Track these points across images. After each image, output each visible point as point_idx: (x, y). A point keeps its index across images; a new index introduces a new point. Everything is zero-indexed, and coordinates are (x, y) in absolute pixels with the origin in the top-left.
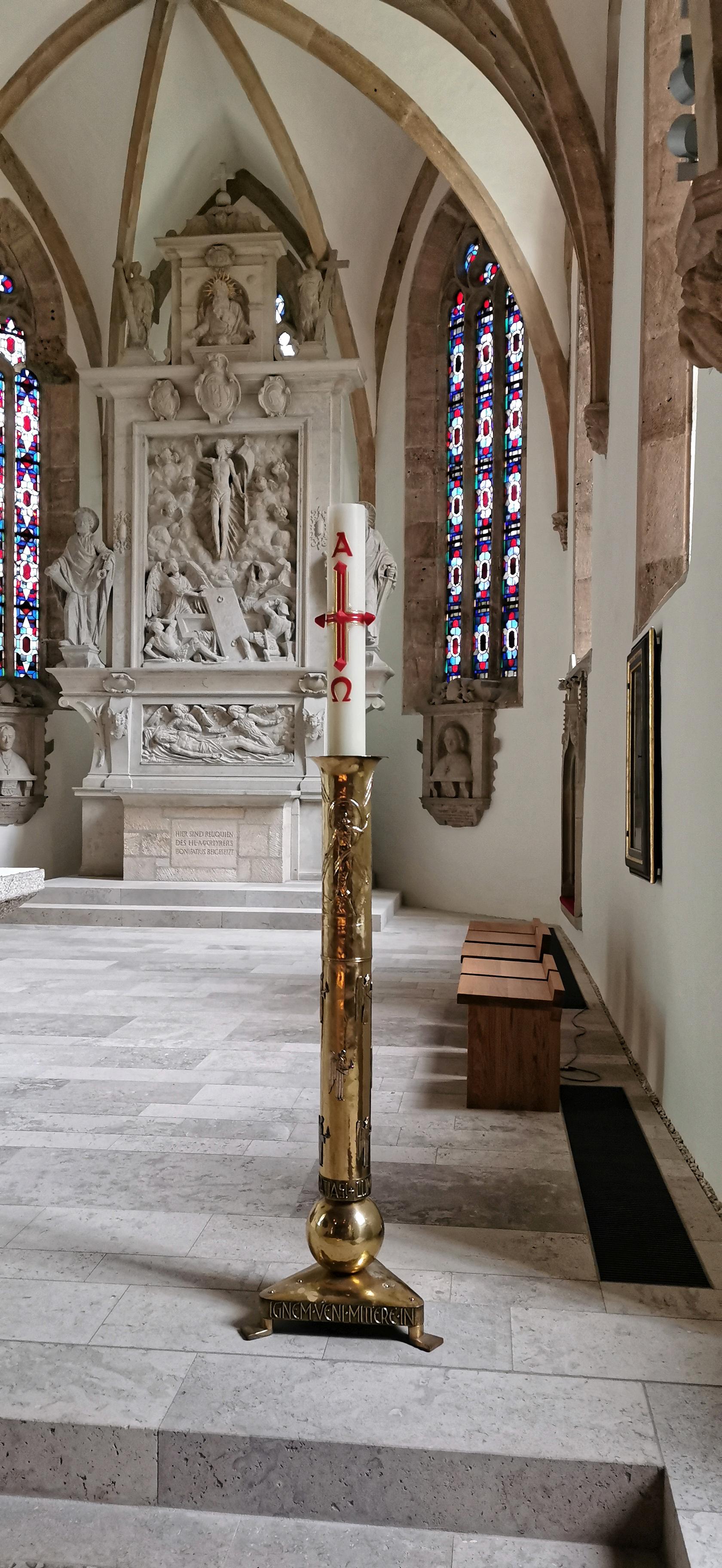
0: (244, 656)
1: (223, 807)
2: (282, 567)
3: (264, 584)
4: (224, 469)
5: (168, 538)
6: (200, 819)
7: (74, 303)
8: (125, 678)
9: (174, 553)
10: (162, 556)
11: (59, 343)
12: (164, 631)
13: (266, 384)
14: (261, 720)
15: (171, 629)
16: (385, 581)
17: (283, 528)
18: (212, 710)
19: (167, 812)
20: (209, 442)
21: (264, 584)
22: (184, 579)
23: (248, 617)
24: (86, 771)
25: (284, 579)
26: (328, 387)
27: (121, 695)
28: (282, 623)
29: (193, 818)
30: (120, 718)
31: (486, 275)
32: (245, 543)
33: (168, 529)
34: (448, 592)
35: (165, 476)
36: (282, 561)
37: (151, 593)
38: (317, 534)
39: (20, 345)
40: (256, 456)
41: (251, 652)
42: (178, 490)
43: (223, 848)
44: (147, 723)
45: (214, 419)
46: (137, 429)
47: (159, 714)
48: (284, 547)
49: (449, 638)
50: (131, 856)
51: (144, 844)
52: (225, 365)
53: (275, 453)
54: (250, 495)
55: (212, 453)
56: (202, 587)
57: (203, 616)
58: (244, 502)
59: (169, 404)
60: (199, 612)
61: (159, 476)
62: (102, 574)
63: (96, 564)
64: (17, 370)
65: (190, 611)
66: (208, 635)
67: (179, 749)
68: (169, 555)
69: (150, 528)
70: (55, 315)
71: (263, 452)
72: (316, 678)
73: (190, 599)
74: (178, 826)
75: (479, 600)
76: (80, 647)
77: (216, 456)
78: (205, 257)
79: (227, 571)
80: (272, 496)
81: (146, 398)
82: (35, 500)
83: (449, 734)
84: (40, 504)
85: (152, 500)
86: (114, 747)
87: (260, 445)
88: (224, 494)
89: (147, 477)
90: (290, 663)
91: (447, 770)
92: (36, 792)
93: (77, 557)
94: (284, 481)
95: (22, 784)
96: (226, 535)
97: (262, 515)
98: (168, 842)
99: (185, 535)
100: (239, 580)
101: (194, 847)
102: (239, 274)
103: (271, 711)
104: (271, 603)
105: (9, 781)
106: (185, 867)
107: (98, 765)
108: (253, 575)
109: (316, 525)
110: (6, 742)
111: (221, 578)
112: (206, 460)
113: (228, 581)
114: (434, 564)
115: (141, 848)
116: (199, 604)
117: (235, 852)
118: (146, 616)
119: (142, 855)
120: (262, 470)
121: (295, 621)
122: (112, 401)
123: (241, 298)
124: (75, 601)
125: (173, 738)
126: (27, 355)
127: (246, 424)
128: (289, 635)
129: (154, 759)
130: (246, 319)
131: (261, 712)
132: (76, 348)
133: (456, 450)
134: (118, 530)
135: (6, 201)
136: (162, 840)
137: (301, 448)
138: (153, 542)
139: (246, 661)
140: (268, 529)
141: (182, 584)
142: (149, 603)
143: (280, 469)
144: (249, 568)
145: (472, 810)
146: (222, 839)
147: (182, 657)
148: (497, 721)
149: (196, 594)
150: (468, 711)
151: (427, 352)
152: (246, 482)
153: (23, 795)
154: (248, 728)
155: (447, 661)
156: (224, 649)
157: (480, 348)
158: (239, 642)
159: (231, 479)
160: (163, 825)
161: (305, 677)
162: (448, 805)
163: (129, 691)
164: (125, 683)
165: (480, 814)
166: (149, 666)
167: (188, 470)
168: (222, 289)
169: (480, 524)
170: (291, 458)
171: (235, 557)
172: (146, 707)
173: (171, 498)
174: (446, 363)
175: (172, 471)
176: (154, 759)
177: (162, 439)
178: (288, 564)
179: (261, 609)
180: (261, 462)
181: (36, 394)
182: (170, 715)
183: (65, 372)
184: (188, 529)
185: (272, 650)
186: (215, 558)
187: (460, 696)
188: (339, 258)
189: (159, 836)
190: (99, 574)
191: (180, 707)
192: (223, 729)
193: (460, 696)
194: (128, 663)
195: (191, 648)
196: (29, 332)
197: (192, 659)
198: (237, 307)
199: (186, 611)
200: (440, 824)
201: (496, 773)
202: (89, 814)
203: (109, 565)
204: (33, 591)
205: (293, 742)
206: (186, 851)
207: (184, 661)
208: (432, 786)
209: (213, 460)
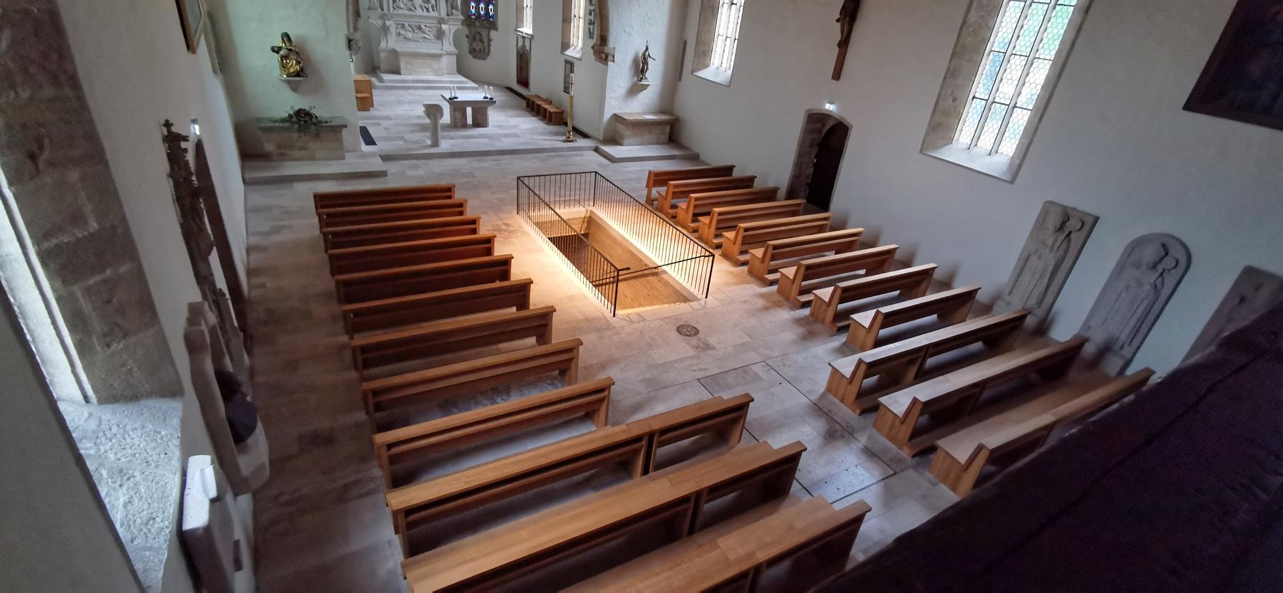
182: (403, 26)
202: (383, 55)
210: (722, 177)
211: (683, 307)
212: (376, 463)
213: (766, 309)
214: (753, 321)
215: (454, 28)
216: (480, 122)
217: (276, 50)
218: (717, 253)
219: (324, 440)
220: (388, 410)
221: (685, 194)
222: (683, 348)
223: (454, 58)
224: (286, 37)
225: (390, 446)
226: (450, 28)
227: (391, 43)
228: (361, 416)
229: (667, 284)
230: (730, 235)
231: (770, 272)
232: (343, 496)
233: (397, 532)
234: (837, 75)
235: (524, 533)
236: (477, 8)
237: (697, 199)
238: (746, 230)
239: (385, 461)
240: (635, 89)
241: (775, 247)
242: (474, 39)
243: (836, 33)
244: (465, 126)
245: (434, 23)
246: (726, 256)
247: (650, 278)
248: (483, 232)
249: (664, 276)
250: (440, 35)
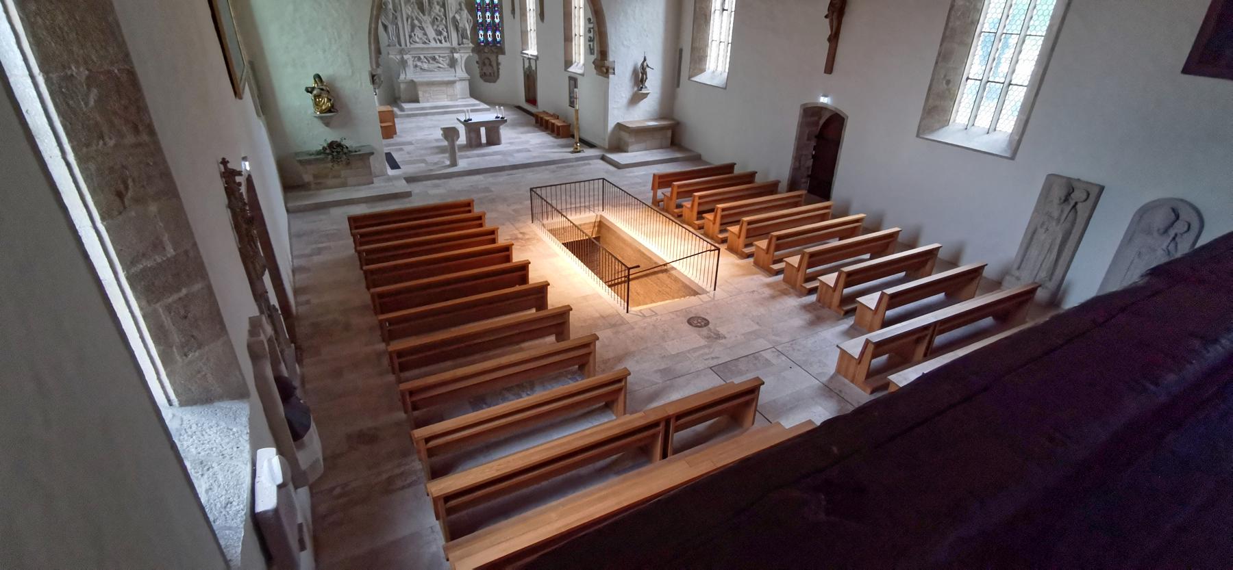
79: (427, 19)
90: (448, 44)
116: (422, 28)
141: (416, 22)
171: (430, 14)
182: (419, 59)
202: (402, 86)
210: (724, 174)
211: (693, 300)
212: (415, 457)
213: (773, 297)
214: (762, 310)
216: (493, 140)
217: (309, 90)
218: (723, 248)
219: (367, 438)
220: (424, 407)
221: (688, 194)
222: (695, 339)
223: (467, 83)
224: (318, 77)
225: (427, 440)
227: (410, 74)
228: (402, 415)
229: (676, 280)
230: (734, 229)
231: (775, 262)
232: (389, 487)
233: (438, 518)
234: (829, 69)
235: (553, 515)
236: (485, 36)
237: (700, 197)
238: (750, 223)
239: (424, 454)
240: (636, 98)
241: (779, 238)
242: (484, 64)
243: (825, 29)
244: (480, 145)
245: (447, 53)
246: (732, 250)
247: (660, 275)
248: (502, 240)
249: (673, 272)
250: (453, 63)
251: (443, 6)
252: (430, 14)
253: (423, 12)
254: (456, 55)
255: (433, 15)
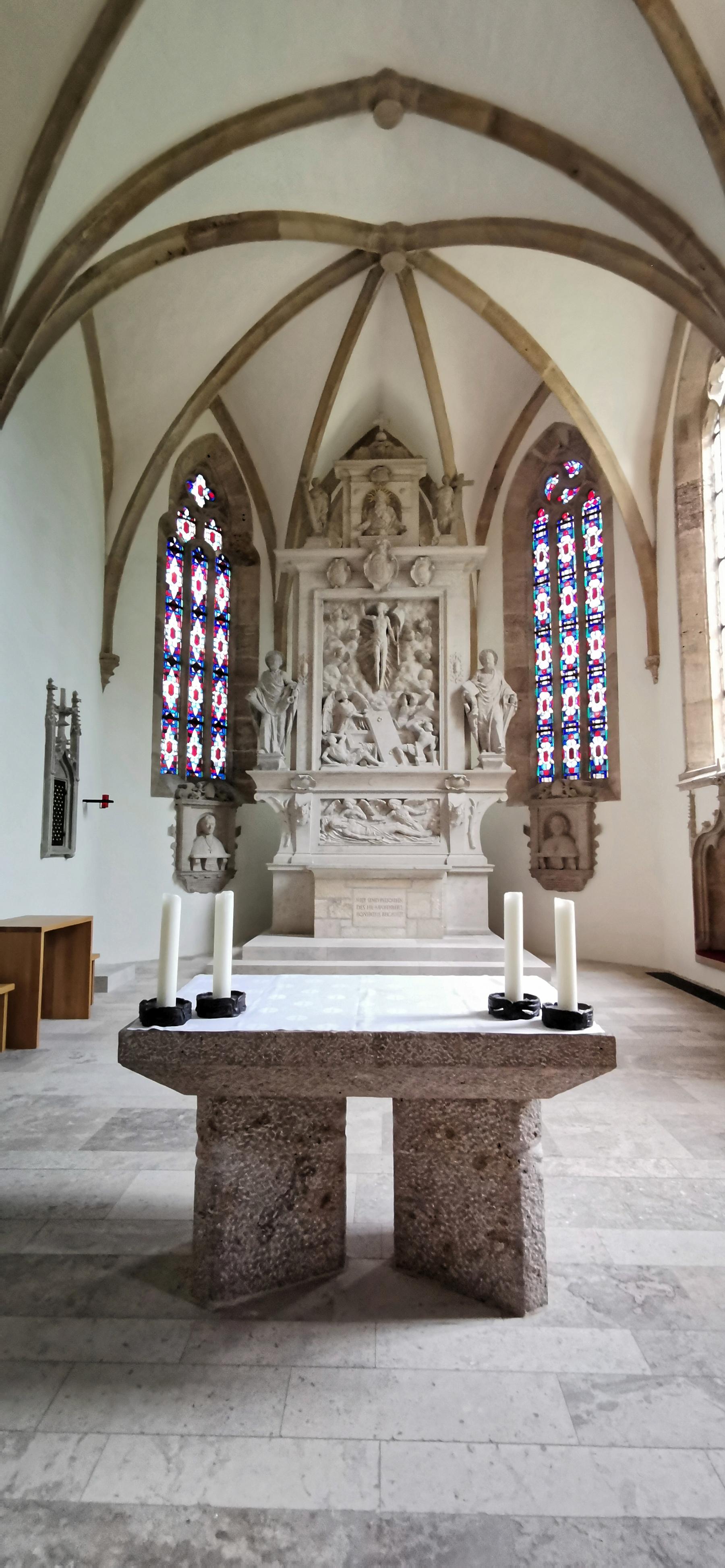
0: (400, 761)
1: (394, 879)
2: (428, 696)
3: (414, 708)
4: (382, 624)
5: (338, 674)
6: (377, 888)
7: (259, 511)
8: (309, 779)
9: (343, 685)
10: (334, 687)
11: (247, 537)
12: (338, 742)
13: (417, 562)
14: (413, 810)
15: (342, 742)
16: (509, 707)
17: (426, 667)
18: (375, 803)
19: (350, 883)
20: (369, 605)
21: (414, 708)
22: (351, 704)
23: (401, 733)
24: (275, 850)
25: (429, 704)
26: (462, 566)
27: (302, 792)
28: (428, 738)
29: (370, 888)
30: (305, 809)
31: (563, 497)
32: (398, 678)
33: (339, 667)
34: (538, 718)
35: (336, 628)
36: (428, 692)
37: (326, 714)
38: (455, 672)
39: (218, 537)
40: (406, 614)
41: (405, 759)
42: (346, 638)
43: (395, 911)
44: (324, 813)
45: (377, 587)
46: (317, 594)
47: (333, 806)
48: (429, 681)
49: (539, 750)
50: (320, 918)
51: (331, 908)
52: (388, 548)
53: (420, 613)
54: (401, 643)
55: (373, 611)
56: (365, 710)
57: (366, 732)
58: (396, 648)
59: (342, 576)
60: (362, 729)
61: (331, 628)
62: (291, 700)
63: (286, 693)
64: (217, 555)
65: (356, 728)
66: (370, 746)
67: (349, 833)
68: (339, 686)
69: (324, 666)
70: (245, 517)
71: (411, 613)
72: (458, 778)
73: (356, 719)
74: (359, 894)
75: (566, 723)
76: (273, 755)
77: (377, 614)
78: (369, 475)
79: (383, 699)
80: (419, 644)
81: (325, 572)
82: (225, 647)
83: (556, 822)
84: (229, 651)
85: (326, 646)
86: (299, 833)
87: (408, 608)
88: (382, 643)
89: (323, 628)
90: (435, 767)
91: (556, 849)
92: (229, 866)
93: (270, 688)
94: (427, 633)
95: (220, 860)
96: (384, 671)
97: (411, 658)
98: (351, 907)
99: (352, 673)
100: (394, 705)
101: (372, 911)
102: (394, 487)
103: (421, 803)
104: (421, 722)
105: (211, 859)
106: (365, 927)
107: (285, 846)
108: (406, 701)
109: (454, 666)
110: (210, 828)
111: (380, 704)
112: (369, 617)
113: (385, 706)
114: (527, 697)
115: (328, 912)
117: (404, 915)
118: (323, 733)
119: (329, 917)
120: (410, 625)
121: (438, 736)
122: (297, 574)
123: (395, 504)
124: (269, 720)
125: (345, 824)
126: (223, 544)
127: (400, 591)
128: (434, 746)
129: (330, 841)
130: (399, 518)
131: (415, 804)
132: (259, 542)
133: (541, 615)
134: (302, 667)
135: (215, 436)
136: (346, 905)
137: (441, 609)
138: (328, 677)
139: (401, 765)
140: (416, 668)
141: (349, 708)
142: (325, 722)
143: (426, 624)
144: (402, 696)
145: (579, 879)
146: (393, 904)
147: (351, 762)
148: (596, 811)
149: (361, 716)
150: (573, 803)
151: (518, 548)
152: (398, 634)
153: (220, 868)
154: (403, 817)
155: (537, 767)
156: (383, 756)
157: (560, 545)
158: (395, 752)
159: (387, 631)
160: (346, 893)
161: (450, 778)
162: (554, 875)
163: (310, 788)
164: (308, 782)
165: (585, 882)
166: (325, 769)
167: (354, 624)
168: (383, 497)
169: (565, 668)
170: (433, 616)
171: (390, 688)
172: (323, 800)
173: (341, 644)
174: (531, 556)
175: (342, 625)
176: (330, 841)
177: (334, 602)
178: (433, 694)
179: (412, 726)
180: (410, 620)
181: (229, 573)
182: (342, 806)
183: (251, 558)
184: (355, 667)
185: (421, 758)
186: (375, 688)
187: (564, 793)
188: (466, 479)
189: (343, 902)
190: (288, 699)
191: (350, 800)
192: (384, 818)
193: (564, 793)
194: (309, 765)
195: (358, 756)
196: (226, 529)
197: (358, 764)
198: (392, 510)
199: (352, 728)
200: (547, 889)
201: (597, 851)
202: (279, 884)
203: (297, 693)
204: (223, 714)
205: (439, 828)
206: (365, 914)
207: (352, 765)
208: (542, 861)
209: (375, 617)
215: (485, 803)
226: (474, 806)
227: (306, 849)
236: (558, 755)
242: (547, 834)
250: (442, 823)
251: (434, 663)
252: (390, 688)
253: (373, 683)
254: (454, 799)
255: (401, 686)
